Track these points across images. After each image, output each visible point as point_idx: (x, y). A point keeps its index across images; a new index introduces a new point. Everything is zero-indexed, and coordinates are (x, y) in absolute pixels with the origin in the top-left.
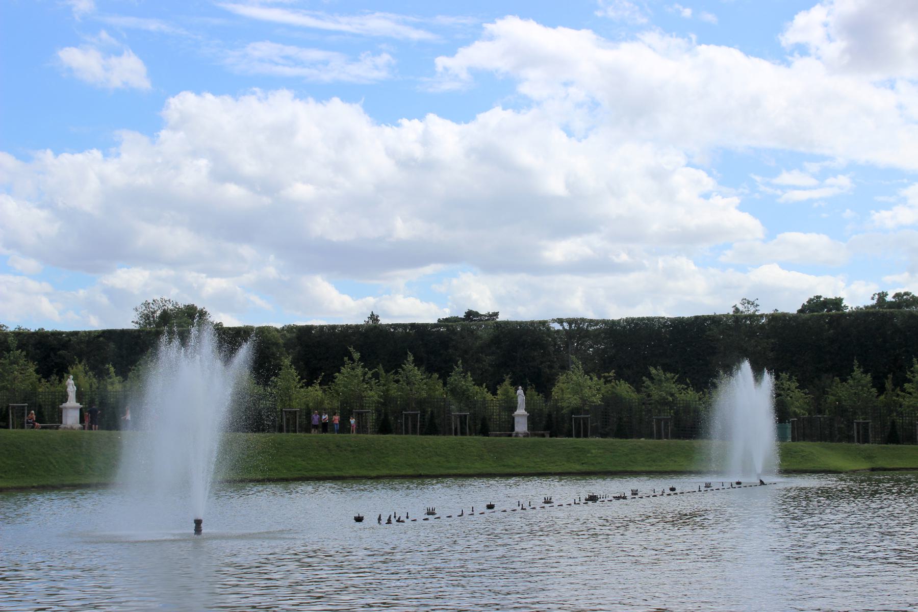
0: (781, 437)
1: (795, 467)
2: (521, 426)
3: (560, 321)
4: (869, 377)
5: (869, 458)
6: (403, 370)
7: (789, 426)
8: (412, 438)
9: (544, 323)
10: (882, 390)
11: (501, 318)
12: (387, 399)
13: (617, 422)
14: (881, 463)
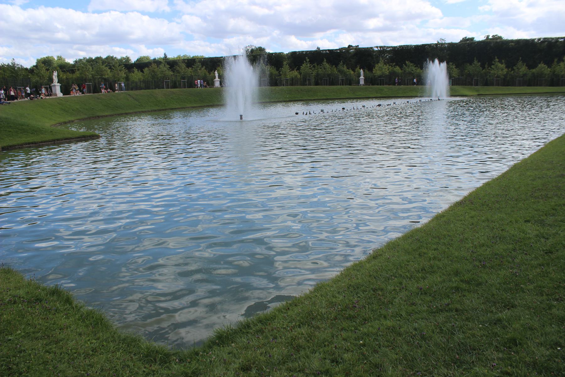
2: (362, 82)
3: (377, 47)
5: (478, 91)
8: (326, 87)
9: (372, 48)
10: (484, 68)
11: (360, 47)
12: (318, 75)
14: (481, 93)
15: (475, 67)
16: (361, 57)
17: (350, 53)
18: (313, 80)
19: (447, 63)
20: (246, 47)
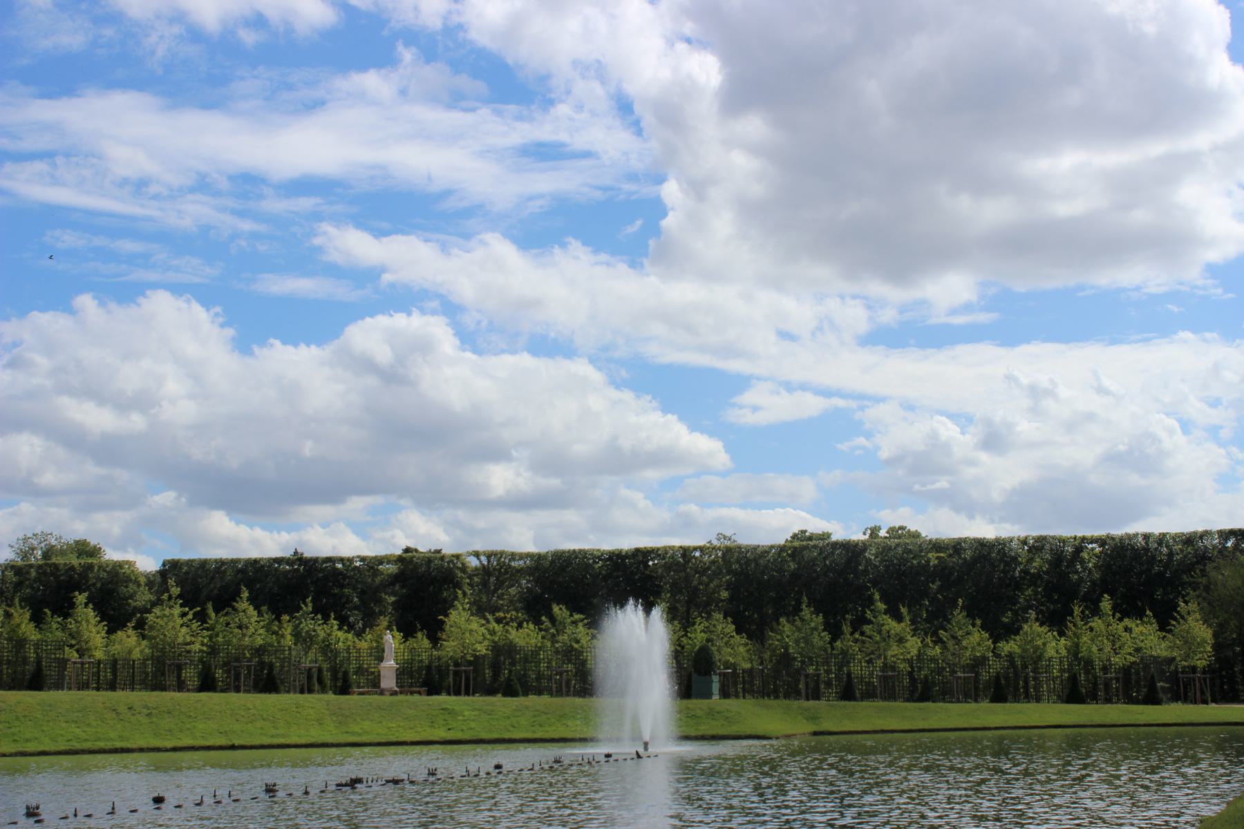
1: (714, 733)
2: (388, 682)
3: (477, 555)
5: (813, 718)
6: (235, 609)
7: (716, 679)
8: (233, 697)
9: (458, 557)
12: (213, 650)
13: (498, 675)
15: (799, 633)
16: (419, 589)
17: (376, 573)
18: (191, 674)
19: (672, 615)
20: (25, 539)
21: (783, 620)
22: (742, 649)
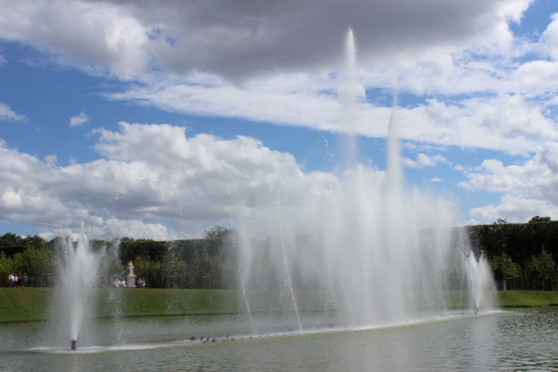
0: (500, 288)
1: (506, 304)
4: (551, 255)
5: (549, 299)
7: (505, 282)
15: (543, 261)
21: (533, 256)
22: (515, 269)
